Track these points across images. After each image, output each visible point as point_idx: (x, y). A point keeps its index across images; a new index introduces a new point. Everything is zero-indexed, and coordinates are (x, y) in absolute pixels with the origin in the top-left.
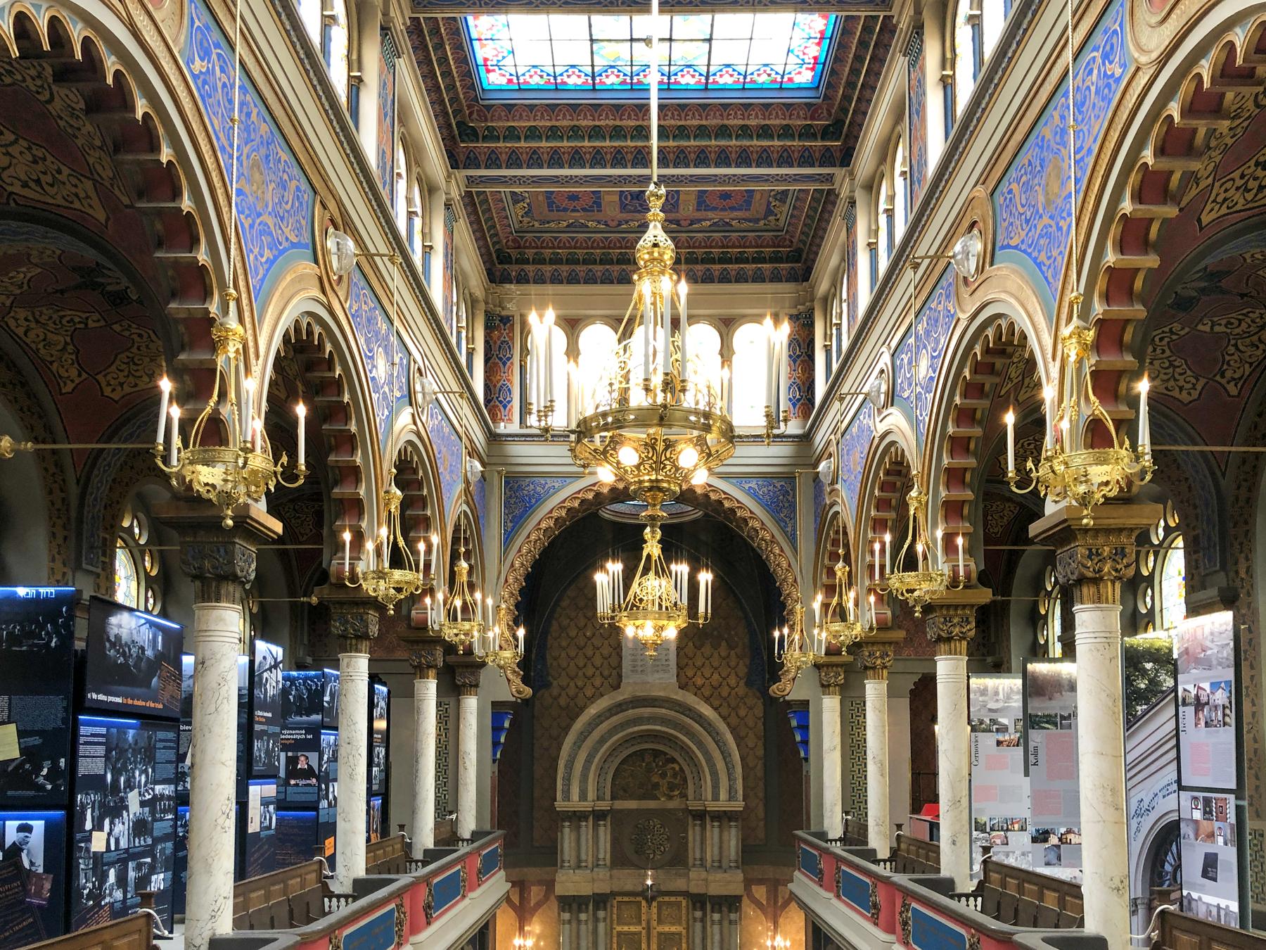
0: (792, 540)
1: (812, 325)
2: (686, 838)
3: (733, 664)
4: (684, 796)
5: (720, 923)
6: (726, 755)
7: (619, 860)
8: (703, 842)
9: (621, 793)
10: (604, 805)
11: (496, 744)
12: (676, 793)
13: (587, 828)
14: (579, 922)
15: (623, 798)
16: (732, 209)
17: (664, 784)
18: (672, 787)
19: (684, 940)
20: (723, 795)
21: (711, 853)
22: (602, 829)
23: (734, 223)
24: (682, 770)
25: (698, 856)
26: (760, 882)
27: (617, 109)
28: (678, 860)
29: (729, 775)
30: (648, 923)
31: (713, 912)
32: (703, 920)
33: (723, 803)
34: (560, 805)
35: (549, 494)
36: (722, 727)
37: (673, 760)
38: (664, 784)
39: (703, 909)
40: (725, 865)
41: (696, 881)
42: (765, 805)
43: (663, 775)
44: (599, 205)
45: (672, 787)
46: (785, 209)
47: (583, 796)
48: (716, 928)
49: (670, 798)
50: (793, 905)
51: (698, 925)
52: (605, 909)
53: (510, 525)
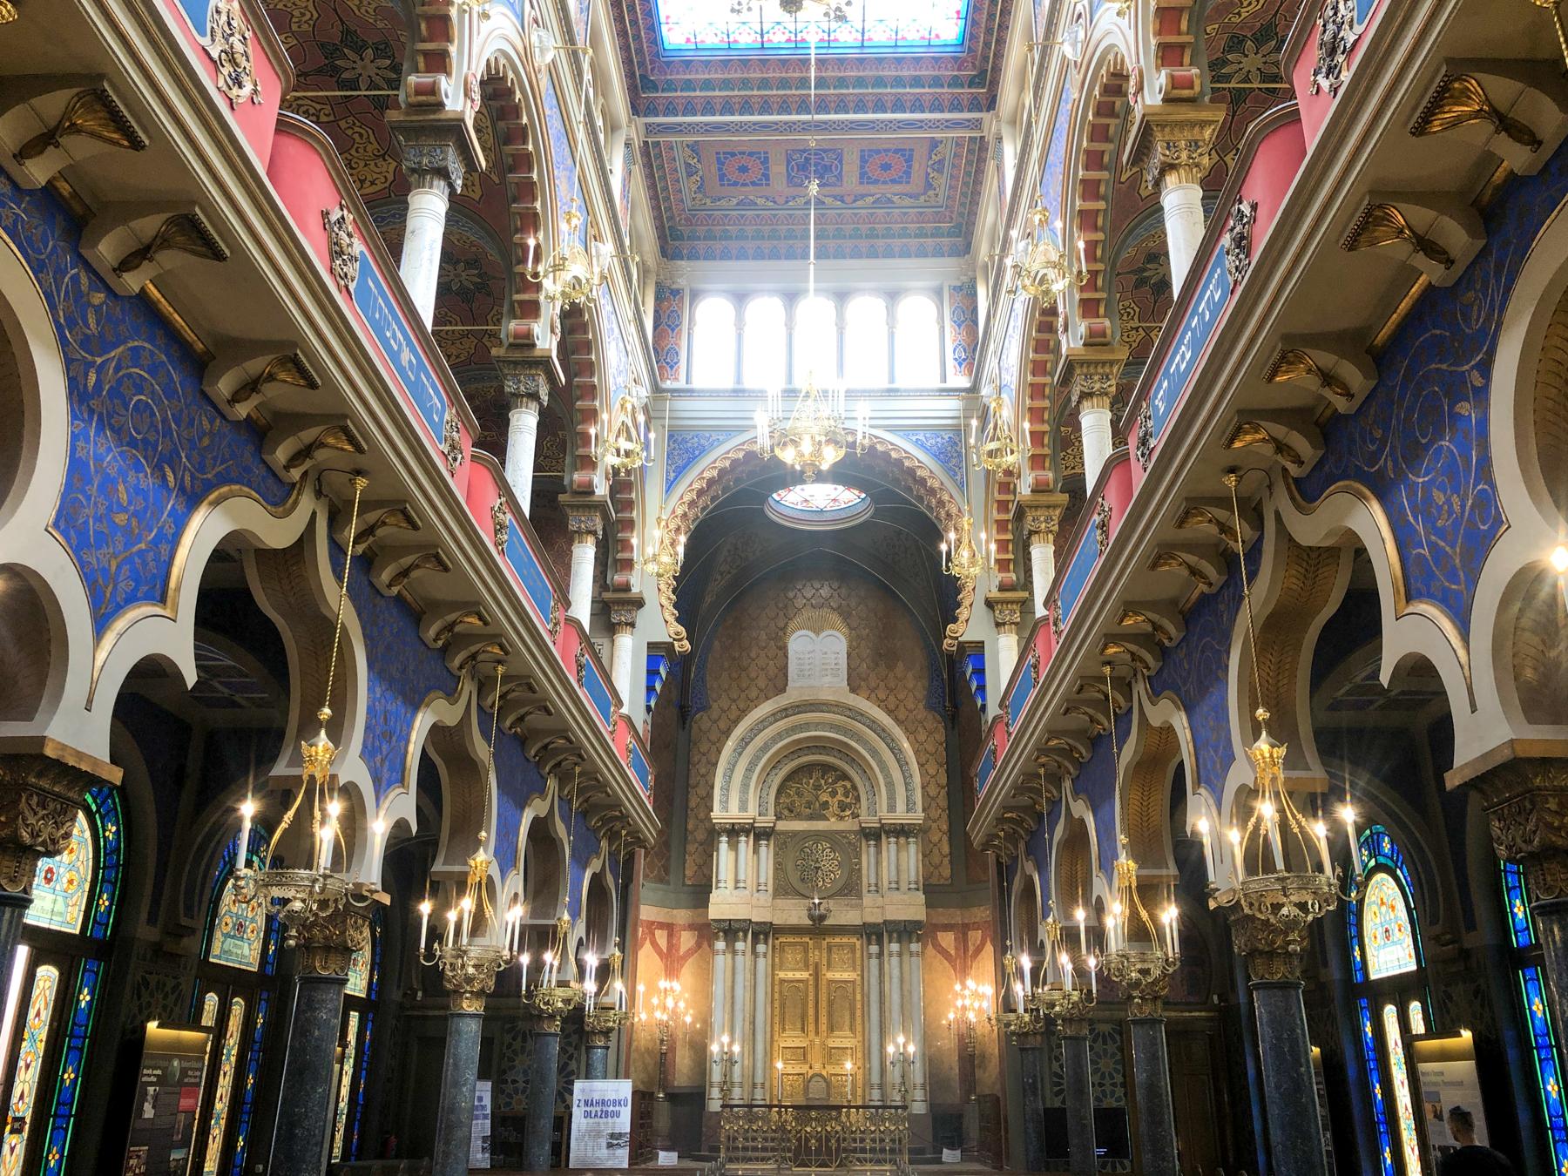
0: (961, 486)
1: (975, 295)
2: (860, 863)
3: (910, 685)
4: (855, 816)
5: (900, 954)
6: (902, 764)
7: (782, 889)
8: (878, 863)
9: (786, 812)
10: (766, 821)
11: (650, 689)
12: (848, 813)
14: (734, 952)
15: (786, 818)
16: (893, 181)
19: (858, 990)
20: (901, 806)
21: (888, 873)
22: (763, 850)
23: (895, 199)
24: (855, 788)
25: (873, 881)
26: (947, 928)
27: (784, 63)
28: (850, 888)
30: (817, 966)
32: (880, 955)
33: (901, 815)
34: (718, 815)
35: (712, 446)
36: (897, 732)
40: (904, 886)
41: (872, 909)
42: (950, 839)
43: (834, 794)
44: (768, 179)
46: (943, 181)
47: (743, 806)
48: (895, 960)
49: (842, 818)
51: (874, 962)
52: (766, 943)
53: (673, 475)
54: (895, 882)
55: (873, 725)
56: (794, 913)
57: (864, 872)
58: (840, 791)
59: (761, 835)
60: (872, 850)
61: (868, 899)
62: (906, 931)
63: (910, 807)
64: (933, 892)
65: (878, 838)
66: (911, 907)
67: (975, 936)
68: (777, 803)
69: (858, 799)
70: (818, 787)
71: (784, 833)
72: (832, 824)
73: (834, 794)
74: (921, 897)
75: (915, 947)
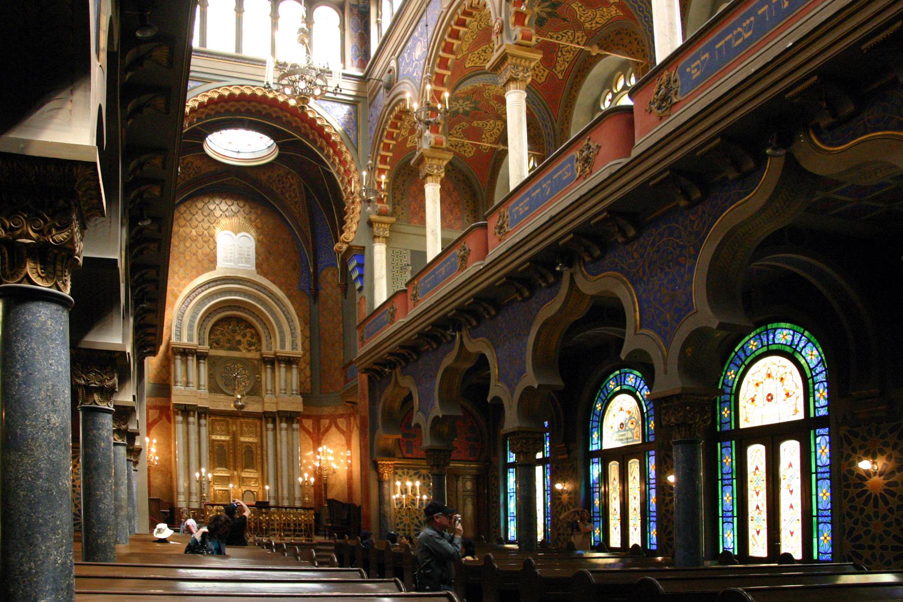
2: (260, 378)
5: (287, 429)
7: (214, 389)
8: (273, 378)
9: (215, 345)
10: (205, 348)
12: (253, 348)
13: (192, 362)
15: (215, 348)
17: (244, 341)
18: (250, 344)
26: (308, 417)
28: (255, 391)
29: (292, 334)
31: (281, 422)
37: (250, 326)
38: (244, 341)
39: (274, 422)
43: (244, 336)
45: (250, 344)
48: (284, 433)
49: (250, 351)
50: (333, 429)
54: (282, 390)
55: (271, 295)
56: (224, 403)
57: (263, 383)
58: (249, 335)
59: (201, 357)
60: (269, 371)
61: (268, 398)
62: (290, 417)
63: (294, 346)
64: (306, 396)
65: (273, 364)
66: (295, 404)
67: (325, 422)
68: (210, 339)
69: (259, 340)
70: (234, 331)
71: (214, 357)
72: (243, 353)
73: (244, 336)
74: (300, 399)
75: (295, 426)
